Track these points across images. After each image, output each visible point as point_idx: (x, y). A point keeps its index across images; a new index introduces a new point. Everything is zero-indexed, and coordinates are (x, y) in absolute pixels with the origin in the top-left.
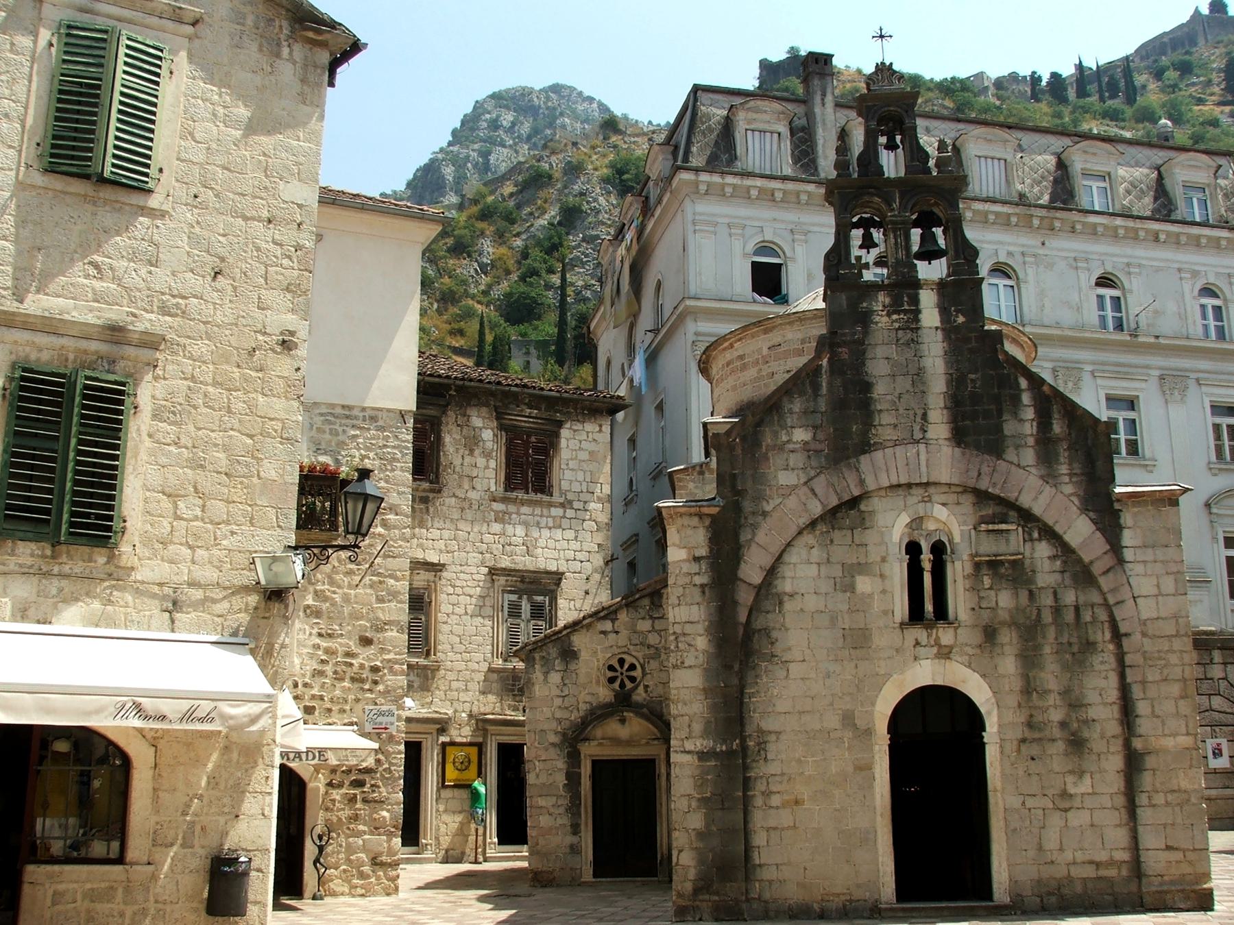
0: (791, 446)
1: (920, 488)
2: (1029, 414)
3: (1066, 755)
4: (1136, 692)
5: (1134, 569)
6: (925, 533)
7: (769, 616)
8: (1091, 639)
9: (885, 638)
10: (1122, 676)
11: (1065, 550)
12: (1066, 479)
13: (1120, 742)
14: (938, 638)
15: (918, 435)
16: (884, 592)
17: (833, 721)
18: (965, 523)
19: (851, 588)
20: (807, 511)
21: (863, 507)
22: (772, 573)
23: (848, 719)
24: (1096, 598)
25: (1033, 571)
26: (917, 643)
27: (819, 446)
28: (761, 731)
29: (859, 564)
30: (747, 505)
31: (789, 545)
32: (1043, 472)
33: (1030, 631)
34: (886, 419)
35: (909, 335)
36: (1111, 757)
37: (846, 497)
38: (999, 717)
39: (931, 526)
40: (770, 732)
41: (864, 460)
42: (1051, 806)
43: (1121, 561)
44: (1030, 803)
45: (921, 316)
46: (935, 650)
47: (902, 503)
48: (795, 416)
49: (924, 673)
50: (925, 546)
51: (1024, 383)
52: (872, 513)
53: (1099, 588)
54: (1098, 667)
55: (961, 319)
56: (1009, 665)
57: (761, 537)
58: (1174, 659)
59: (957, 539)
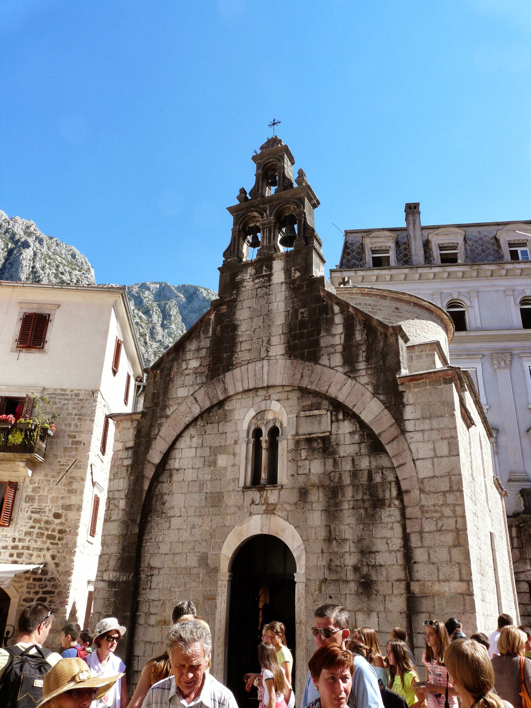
0: (187, 372)
1: (265, 391)
2: (339, 329)
3: (357, 594)
4: (414, 541)
6: (265, 422)
7: (165, 485)
8: (381, 496)
9: (232, 500)
10: (404, 527)
11: (363, 427)
12: (363, 372)
13: (403, 585)
14: (267, 497)
15: (263, 354)
18: (291, 412)
19: (214, 463)
20: (191, 412)
21: (226, 408)
22: (167, 456)
24: (384, 462)
25: (338, 445)
26: (253, 502)
27: (203, 369)
29: (221, 446)
31: (179, 436)
32: (347, 369)
33: (333, 492)
34: (245, 346)
36: (394, 599)
37: (215, 402)
39: (270, 416)
40: (155, 568)
41: (228, 375)
43: (403, 432)
45: (272, 277)
47: (251, 402)
50: (265, 432)
52: (231, 411)
54: (385, 519)
55: (298, 274)
56: (316, 518)
57: (163, 432)
59: (285, 424)
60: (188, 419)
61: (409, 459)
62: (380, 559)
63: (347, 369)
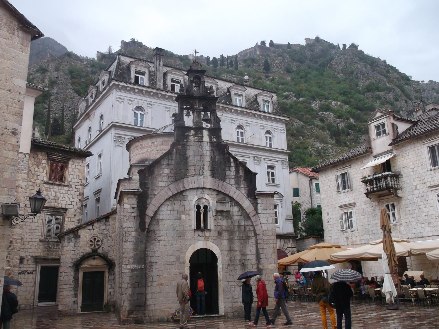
2: (233, 169)
3: (241, 269)
4: (261, 251)
5: (261, 216)
7: (155, 226)
9: (190, 234)
10: (257, 247)
11: (242, 209)
12: (243, 189)
14: (205, 234)
15: (201, 173)
16: (189, 220)
17: (173, 259)
19: (179, 219)
21: (184, 194)
22: (156, 213)
23: (178, 258)
24: (250, 223)
25: (233, 215)
26: (199, 236)
28: (151, 262)
30: (150, 192)
31: (162, 205)
33: (231, 233)
34: (192, 168)
35: (200, 143)
38: (222, 258)
41: (185, 180)
42: (236, 285)
43: (257, 213)
44: (230, 284)
46: (204, 238)
48: (165, 166)
49: (200, 245)
51: (232, 160)
53: (251, 221)
54: (250, 244)
55: (215, 140)
56: (225, 242)
57: (153, 202)
58: (271, 242)
59: (211, 205)
60: (166, 197)
61: (259, 223)
62: (249, 257)
63: (237, 186)
